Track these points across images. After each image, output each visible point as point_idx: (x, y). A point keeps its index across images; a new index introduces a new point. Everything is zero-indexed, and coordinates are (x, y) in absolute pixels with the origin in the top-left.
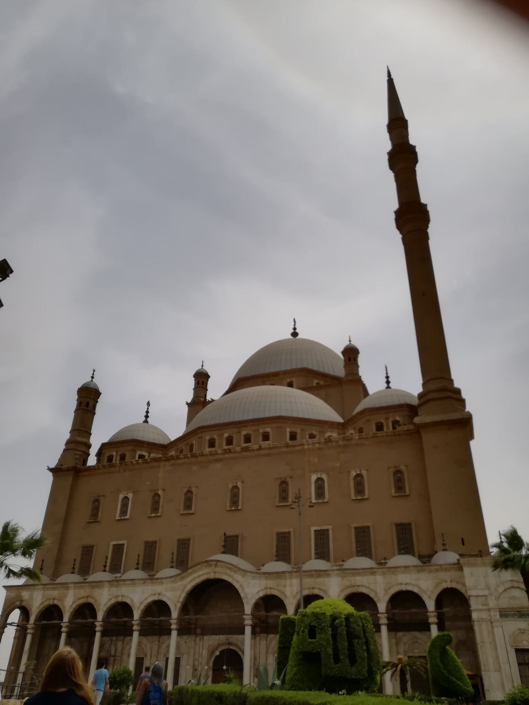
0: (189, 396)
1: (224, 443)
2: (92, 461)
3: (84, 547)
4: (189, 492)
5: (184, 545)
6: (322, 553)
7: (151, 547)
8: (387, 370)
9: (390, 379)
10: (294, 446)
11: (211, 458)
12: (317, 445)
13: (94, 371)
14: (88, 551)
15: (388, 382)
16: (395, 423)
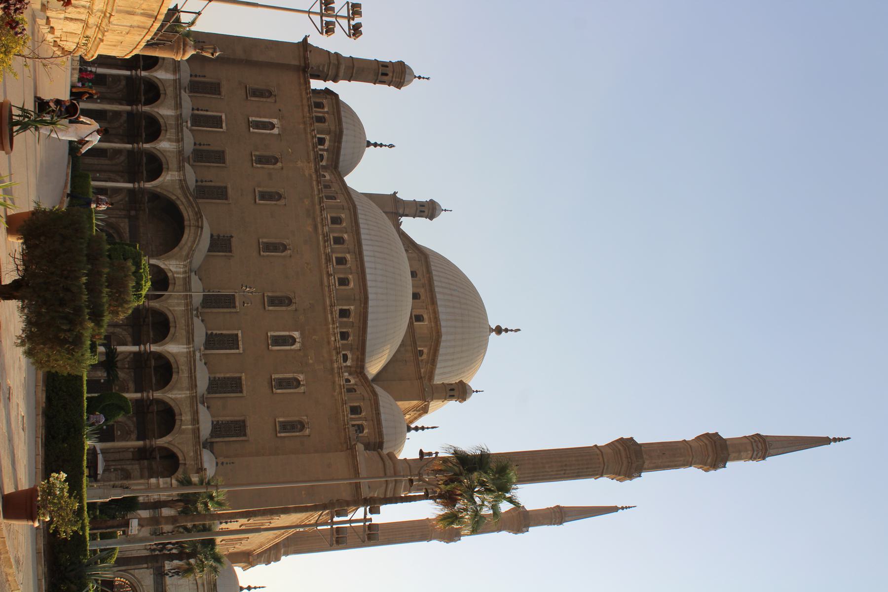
0: (403, 196)
1: (336, 235)
2: (316, 84)
3: (219, 84)
4: (279, 197)
5: (221, 193)
6: (212, 341)
7: (219, 157)
8: (433, 428)
9: (420, 431)
10: (332, 313)
11: (319, 219)
12: (333, 339)
13: (428, 79)
14: (214, 89)
15: (416, 429)
16: (360, 428)
